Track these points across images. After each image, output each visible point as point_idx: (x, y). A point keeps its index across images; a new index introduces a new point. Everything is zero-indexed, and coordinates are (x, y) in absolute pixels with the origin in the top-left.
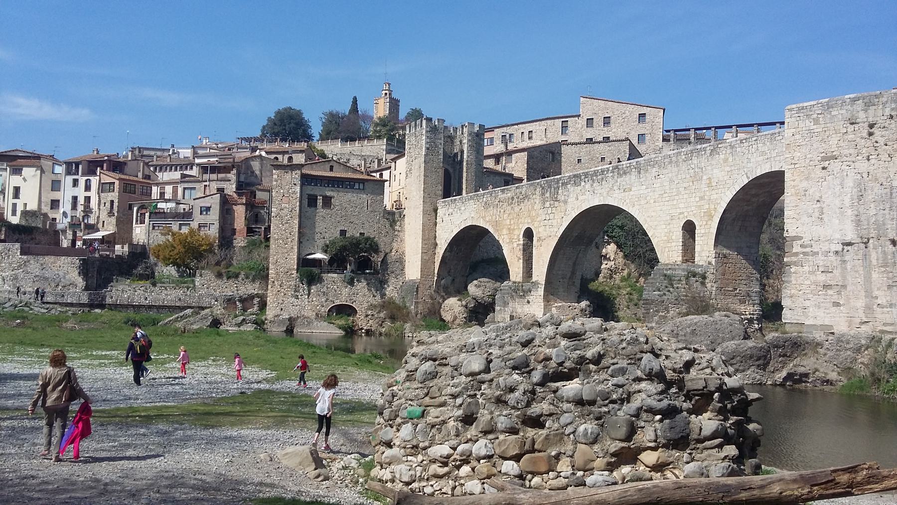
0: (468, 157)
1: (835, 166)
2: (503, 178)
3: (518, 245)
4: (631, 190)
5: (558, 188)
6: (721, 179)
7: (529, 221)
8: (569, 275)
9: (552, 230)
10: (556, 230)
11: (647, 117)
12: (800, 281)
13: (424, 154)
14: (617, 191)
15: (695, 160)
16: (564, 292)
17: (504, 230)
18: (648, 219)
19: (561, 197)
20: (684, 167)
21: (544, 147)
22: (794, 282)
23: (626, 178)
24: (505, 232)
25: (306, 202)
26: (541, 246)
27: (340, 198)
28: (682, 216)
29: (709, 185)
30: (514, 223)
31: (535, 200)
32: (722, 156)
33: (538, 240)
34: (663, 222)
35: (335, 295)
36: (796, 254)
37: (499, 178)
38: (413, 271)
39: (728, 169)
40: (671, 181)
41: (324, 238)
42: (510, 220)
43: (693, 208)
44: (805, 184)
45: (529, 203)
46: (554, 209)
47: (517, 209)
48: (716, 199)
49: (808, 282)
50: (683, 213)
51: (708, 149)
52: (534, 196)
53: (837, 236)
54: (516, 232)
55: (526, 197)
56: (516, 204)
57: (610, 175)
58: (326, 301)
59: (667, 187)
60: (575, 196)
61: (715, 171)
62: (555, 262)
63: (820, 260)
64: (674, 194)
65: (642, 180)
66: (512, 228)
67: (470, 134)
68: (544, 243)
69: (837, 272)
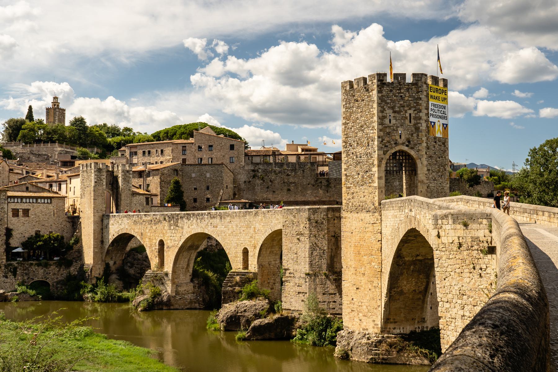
0: (122, 185)
1: (302, 238)
2: (145, 196)
3: (155, 249)
5: (178, 219)
6: (260, 229)
7: (162, 236)
8: (186, 267)
9: (175, 243)
10: (177, 243)
11: (235, 147)
12: (289, 290)
13: (93, 185)
14: (210, 227)
15: (248, 217)
16: (183, 276)
17: (147, 239)
18: (226, 244)
20: (242, 219)
21: (171, 167)
22: (287, 290)
23: (215, 220)
24: (147, 240)
25: (10, 214)
27: (36, 209)
28: (242, 245)
29: (254, 231)
30: (153, 235)
32: (260, 217)
35: (34, 275)
36: (288, 277)
37: (142, 197)
38: (89, 258)
39: (262, 224)
40: (237, 226)
41: (24, 237)
43: (247, 242)
44: (291, 245)
45: (161, 225)
47: (154, 227)
48: (258, 239)
49: (292, 290)
50: (242, 243)
53: (303, 270)
54: (154, 241)
55: (160, 221)
58: (28, 279)
59: (235, 229)
61: (257, 224)
62: (177, 260)
63: (297, 281)
64: (238, 233)
65: (223, 222)
67: (123, 171)
68: (171, 250)
69: (303, 286)
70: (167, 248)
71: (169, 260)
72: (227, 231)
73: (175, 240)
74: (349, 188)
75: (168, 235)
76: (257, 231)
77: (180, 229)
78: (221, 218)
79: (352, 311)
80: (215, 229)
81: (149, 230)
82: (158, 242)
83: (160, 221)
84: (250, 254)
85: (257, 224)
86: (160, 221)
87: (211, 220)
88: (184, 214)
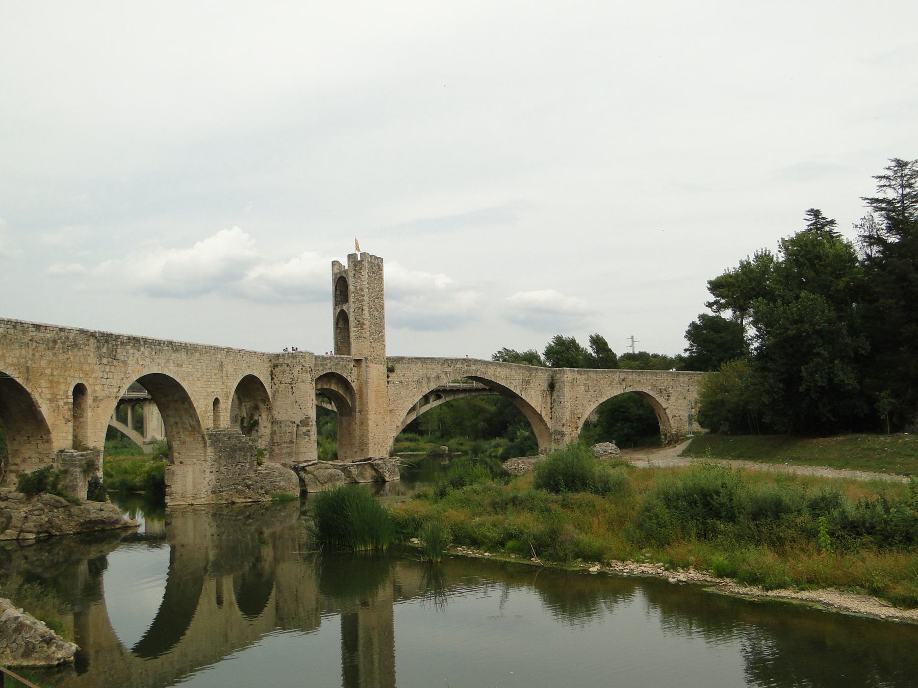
3: (66, 403)
4: (181, 366)
5: (117, 345)
9: (111, 390)
10: (116, 390)
14: (172, 365)
18: (194, 393)
19: (120, 357)
24: (44, 383)
26: (98, 407)
28: (213, 394)
31: (89, 352)
33: (94, 400)
34: (202, 397)
40: (207, 367)
42: (52, 369)
43: (219, 390)
45: (81, 353)
46: (113, 368)
47: (62, 357)
48: (230, 386)
50: (213, 392)
51: (225, 350)
52: (87, 347)
56: (61, 351)
57: (167, 348)
60: (135, 359)
65: (189, 360)
66: (55, 379)
68: (102, 405)
70: (95, 399)
71: (99, 426)
72: (196, 373)
73: (110, 386)
74: (371, 342)
75: (95, 375)
76: (229, 375)
77: (122, 365)
78: (187, 354)
79: (375, 444)
80: (180, 368)
81: (50, 362)
82: (72, 389)
83: (75, 345)
84: (222, 405)
85: (229, 366)
86: (76, 345)
87: (173, 355)
88: (129, 338)
